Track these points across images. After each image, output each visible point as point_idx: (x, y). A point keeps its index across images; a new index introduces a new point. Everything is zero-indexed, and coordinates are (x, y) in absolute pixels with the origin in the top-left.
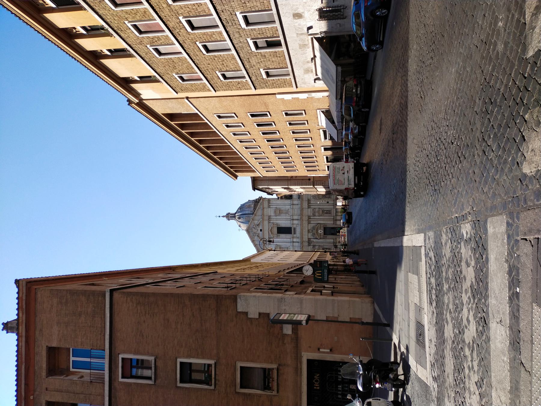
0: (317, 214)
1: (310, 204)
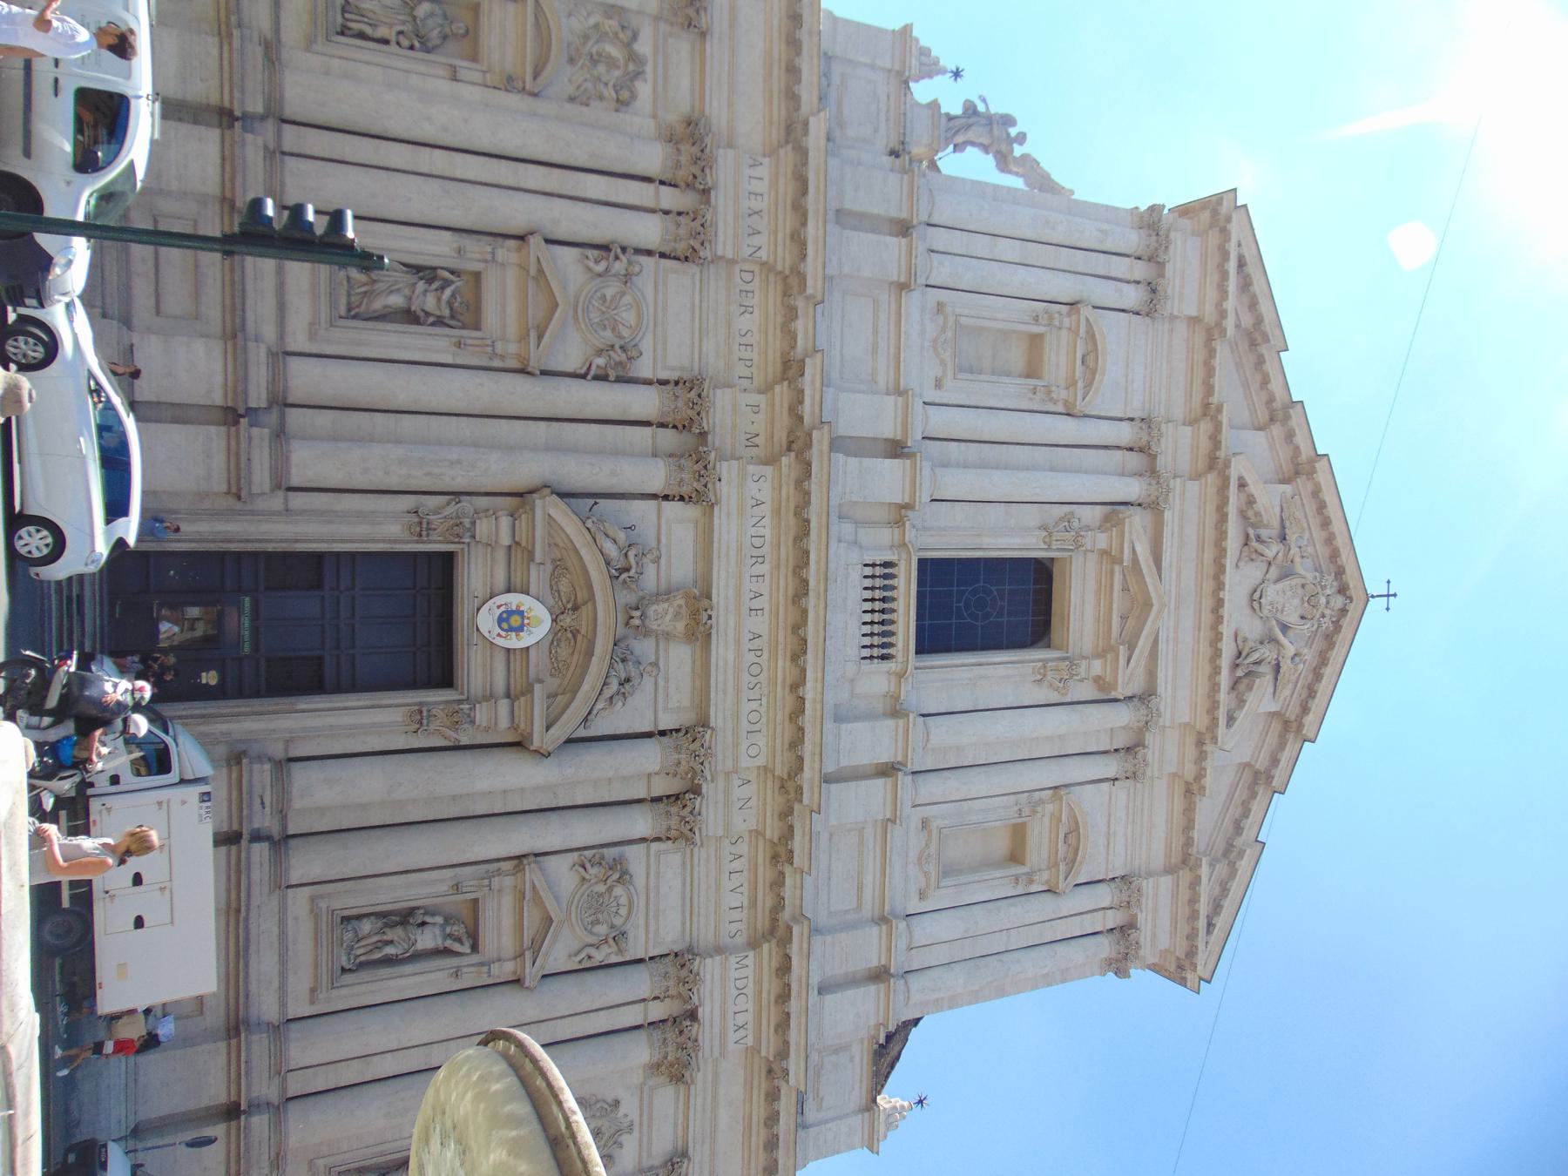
0: (562, 872)
1: (657, 1011)
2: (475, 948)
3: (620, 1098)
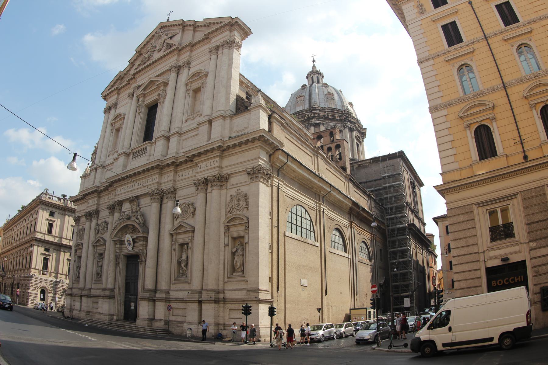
2: (187, 244)
3: (230, 195)
